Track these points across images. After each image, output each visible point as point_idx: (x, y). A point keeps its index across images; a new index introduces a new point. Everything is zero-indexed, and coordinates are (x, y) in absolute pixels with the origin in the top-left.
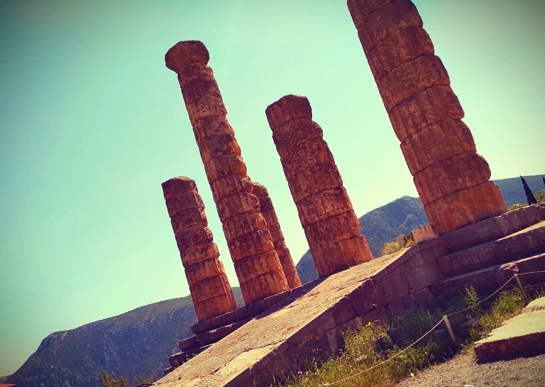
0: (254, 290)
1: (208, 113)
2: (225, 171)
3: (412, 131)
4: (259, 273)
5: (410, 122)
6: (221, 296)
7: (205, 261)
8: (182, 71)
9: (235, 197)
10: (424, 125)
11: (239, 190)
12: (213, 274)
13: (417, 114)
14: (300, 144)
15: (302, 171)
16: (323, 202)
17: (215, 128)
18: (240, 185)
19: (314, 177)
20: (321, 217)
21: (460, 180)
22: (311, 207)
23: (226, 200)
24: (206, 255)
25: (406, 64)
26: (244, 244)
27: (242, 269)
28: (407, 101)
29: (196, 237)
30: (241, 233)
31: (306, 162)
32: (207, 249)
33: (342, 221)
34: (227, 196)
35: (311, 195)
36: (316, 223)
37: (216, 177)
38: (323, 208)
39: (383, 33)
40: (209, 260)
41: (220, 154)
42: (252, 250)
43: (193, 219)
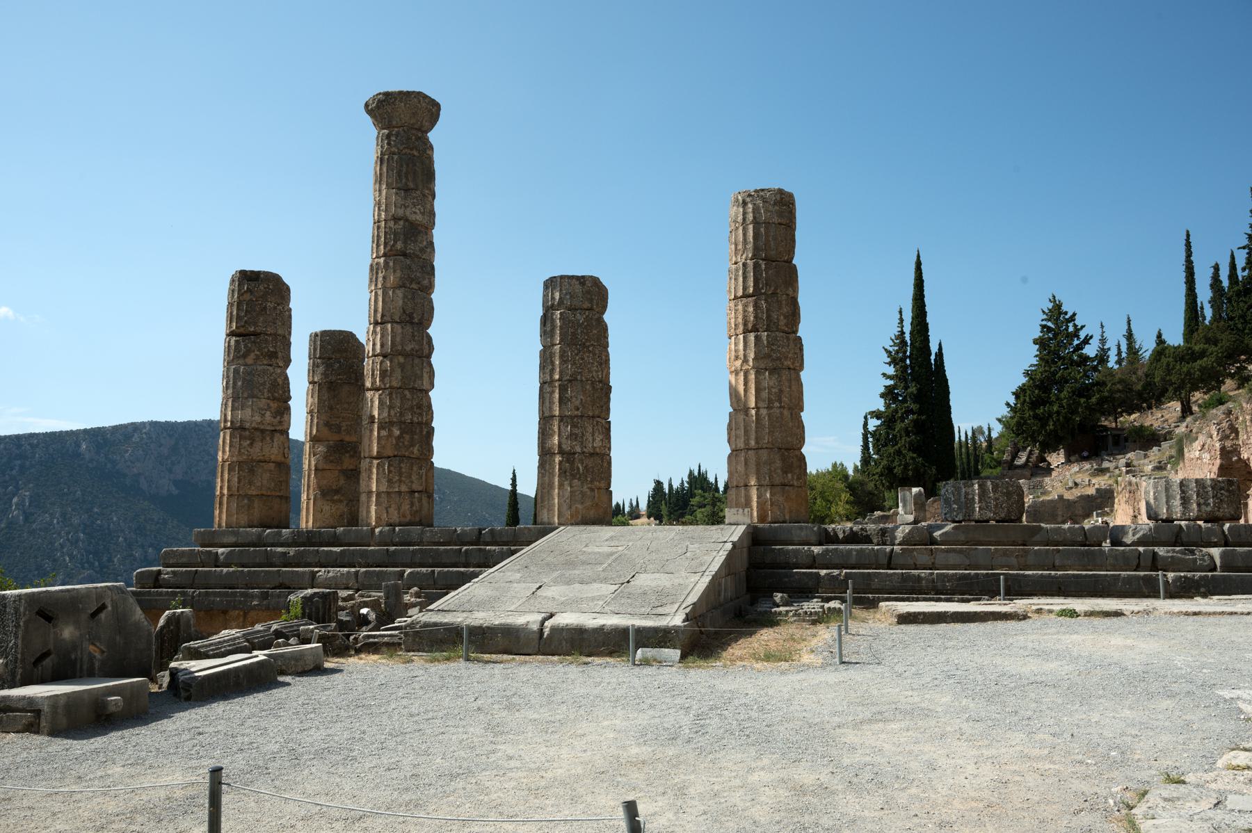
0: (399, 509)
1: (419, 217)
4: (416, 487)
5: (765, 394)
6: (281, 497)
9: (417, 361)
10: (777, 404)
12: (280, 458)
22: (576, 431)
23: (401, 359)
24: (280, 422)
26: (407, 437)
29: (274, 385)
30: (408, 417)
38: (590, 439)
42: (415, 451)
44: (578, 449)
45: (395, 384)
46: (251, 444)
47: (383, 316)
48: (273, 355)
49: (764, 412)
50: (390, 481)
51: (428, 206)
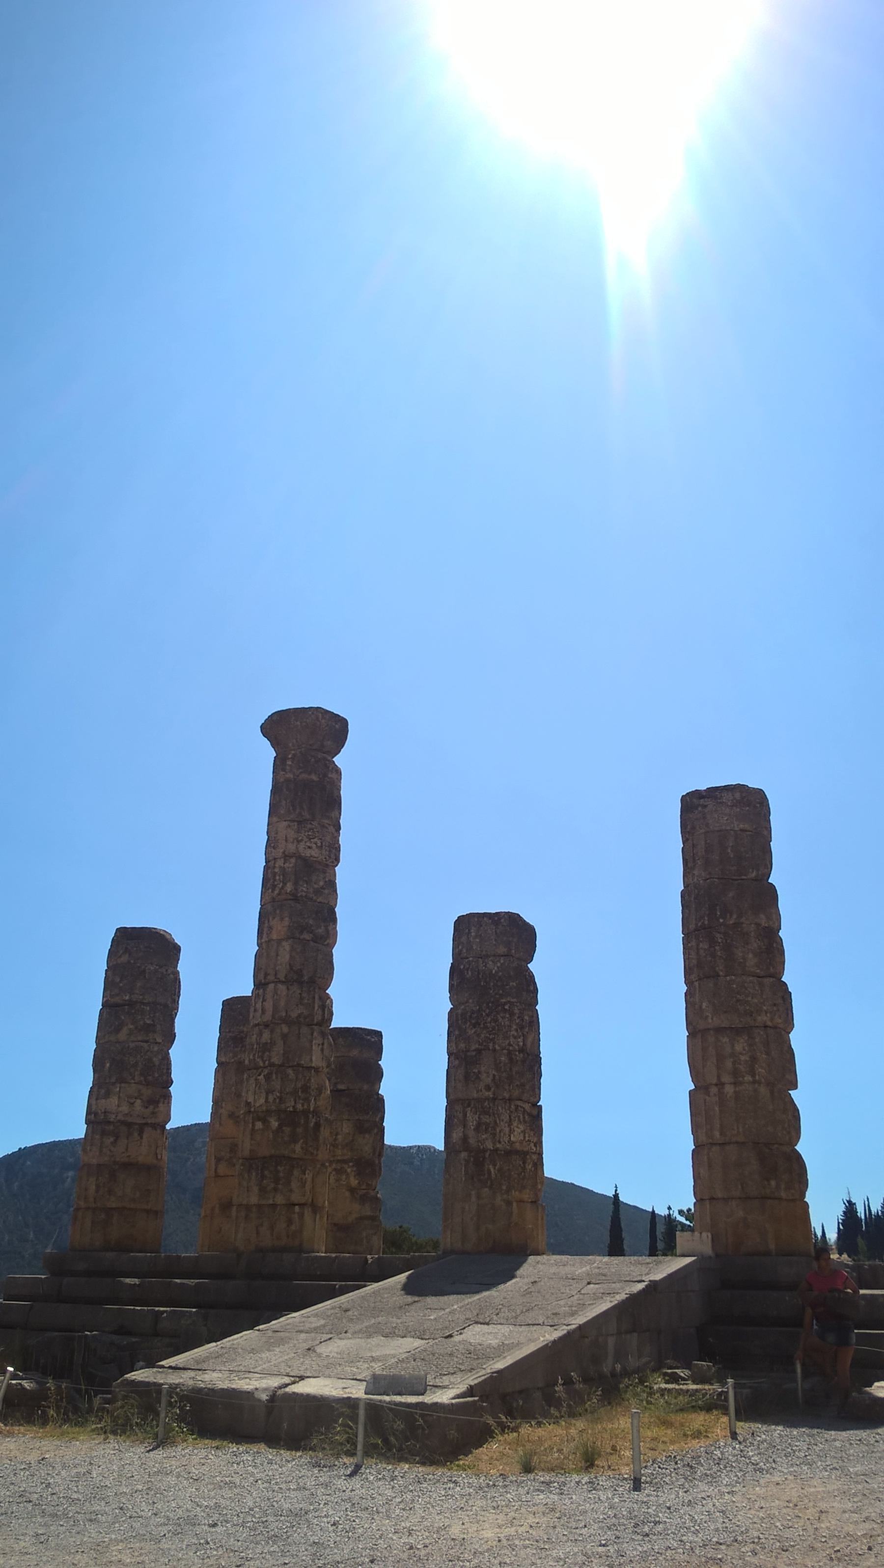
1: (314, 853)
2: (305, 972)
3: (726, 1079)
4: (296, 1197)
5: (729, 1064)
6: (148, 1212)
7: (146, 1124)
8: (294, 755)
9: (305, 1030)
10: (748, 1078)
11: (315, 1021)
13: (743, 1058)
14: (505, 1004)
15: (494, 1050)
16: (510, 1119)
17: (316, 886)
18: (320, 1012)
19: (511, 1069)
20: (498, 1146)
21: (773, 1183)
22: (486, 1119)
23: (285, 1029)
24: (153, 1113)
25: (751, 978)
26: (287, 1130)
27: (263, 1177)
28: (737, 1032)
30: (290, 1104)
31: (506, 1037)
32: (158, 1102)
33: (529, 1167)
34: (287, 1021)
35: (494, 1099)
36: (485, 1151)
37: (281, 976)
38: (507, 1130)
39: (731, 916)
40: (154, 1126)
41: (306, 936)
42: (298, 1148)
43: (158, 1027)
44: (489, 1145)
45: (276, 1060)
46: (114, 1143)
47: (266, 975)
48: (148, 1029)
49: (729, 1090)
50: (263, 1190)
51: (328, 838)
